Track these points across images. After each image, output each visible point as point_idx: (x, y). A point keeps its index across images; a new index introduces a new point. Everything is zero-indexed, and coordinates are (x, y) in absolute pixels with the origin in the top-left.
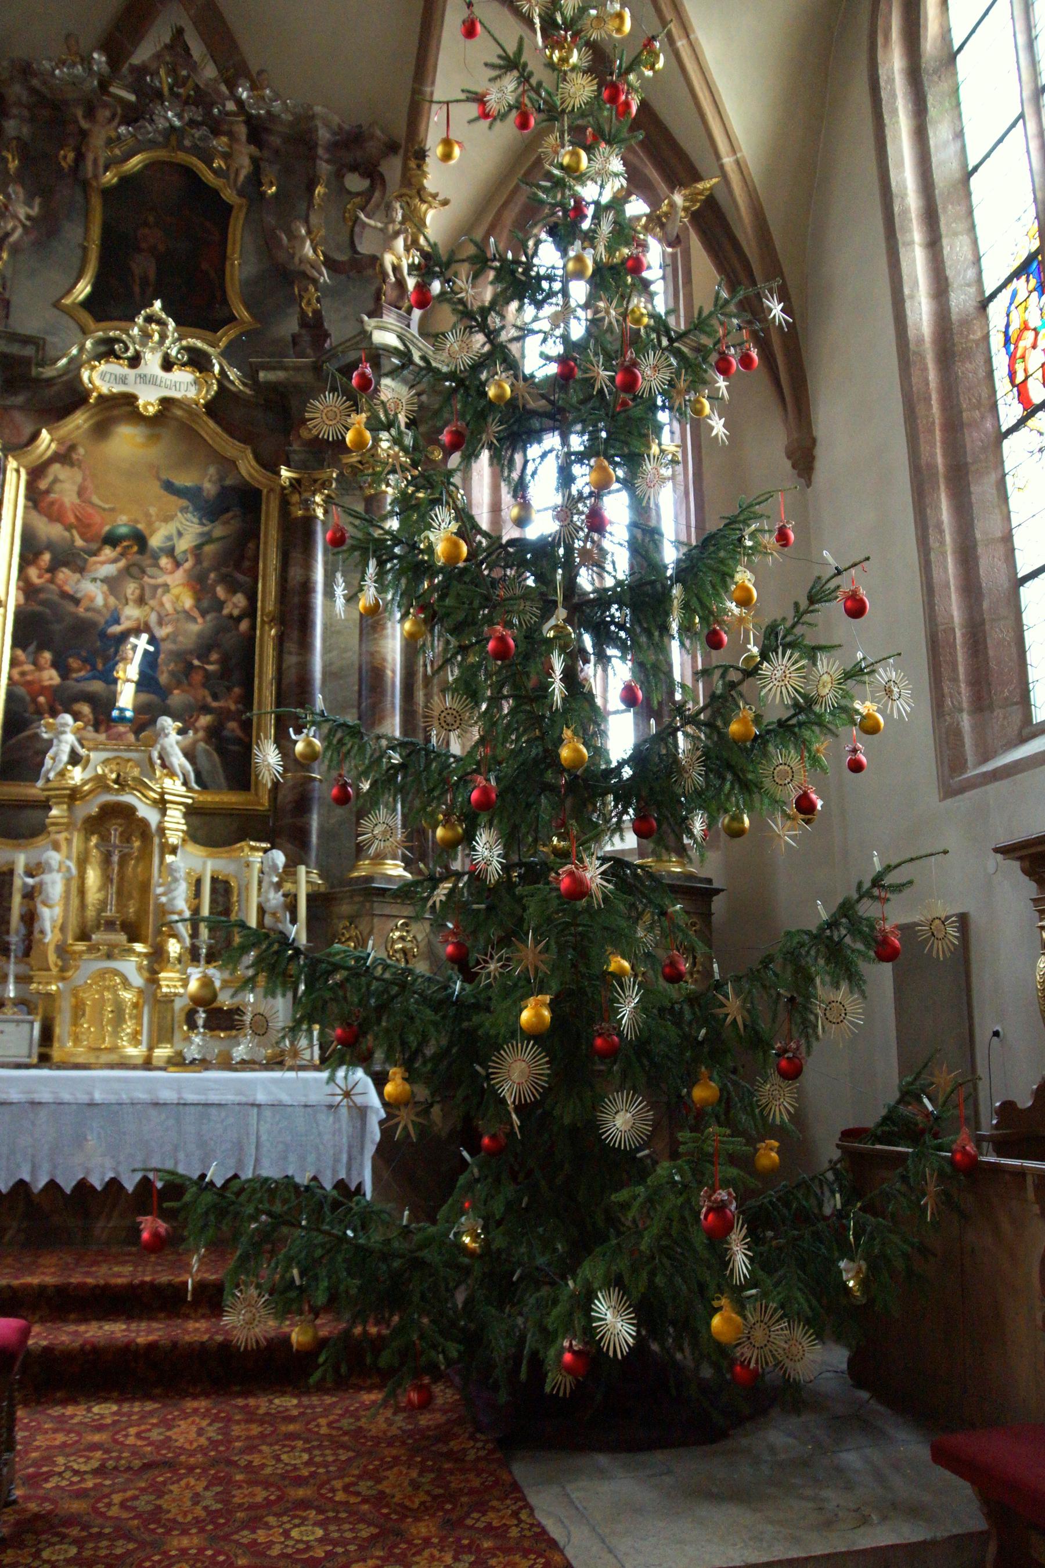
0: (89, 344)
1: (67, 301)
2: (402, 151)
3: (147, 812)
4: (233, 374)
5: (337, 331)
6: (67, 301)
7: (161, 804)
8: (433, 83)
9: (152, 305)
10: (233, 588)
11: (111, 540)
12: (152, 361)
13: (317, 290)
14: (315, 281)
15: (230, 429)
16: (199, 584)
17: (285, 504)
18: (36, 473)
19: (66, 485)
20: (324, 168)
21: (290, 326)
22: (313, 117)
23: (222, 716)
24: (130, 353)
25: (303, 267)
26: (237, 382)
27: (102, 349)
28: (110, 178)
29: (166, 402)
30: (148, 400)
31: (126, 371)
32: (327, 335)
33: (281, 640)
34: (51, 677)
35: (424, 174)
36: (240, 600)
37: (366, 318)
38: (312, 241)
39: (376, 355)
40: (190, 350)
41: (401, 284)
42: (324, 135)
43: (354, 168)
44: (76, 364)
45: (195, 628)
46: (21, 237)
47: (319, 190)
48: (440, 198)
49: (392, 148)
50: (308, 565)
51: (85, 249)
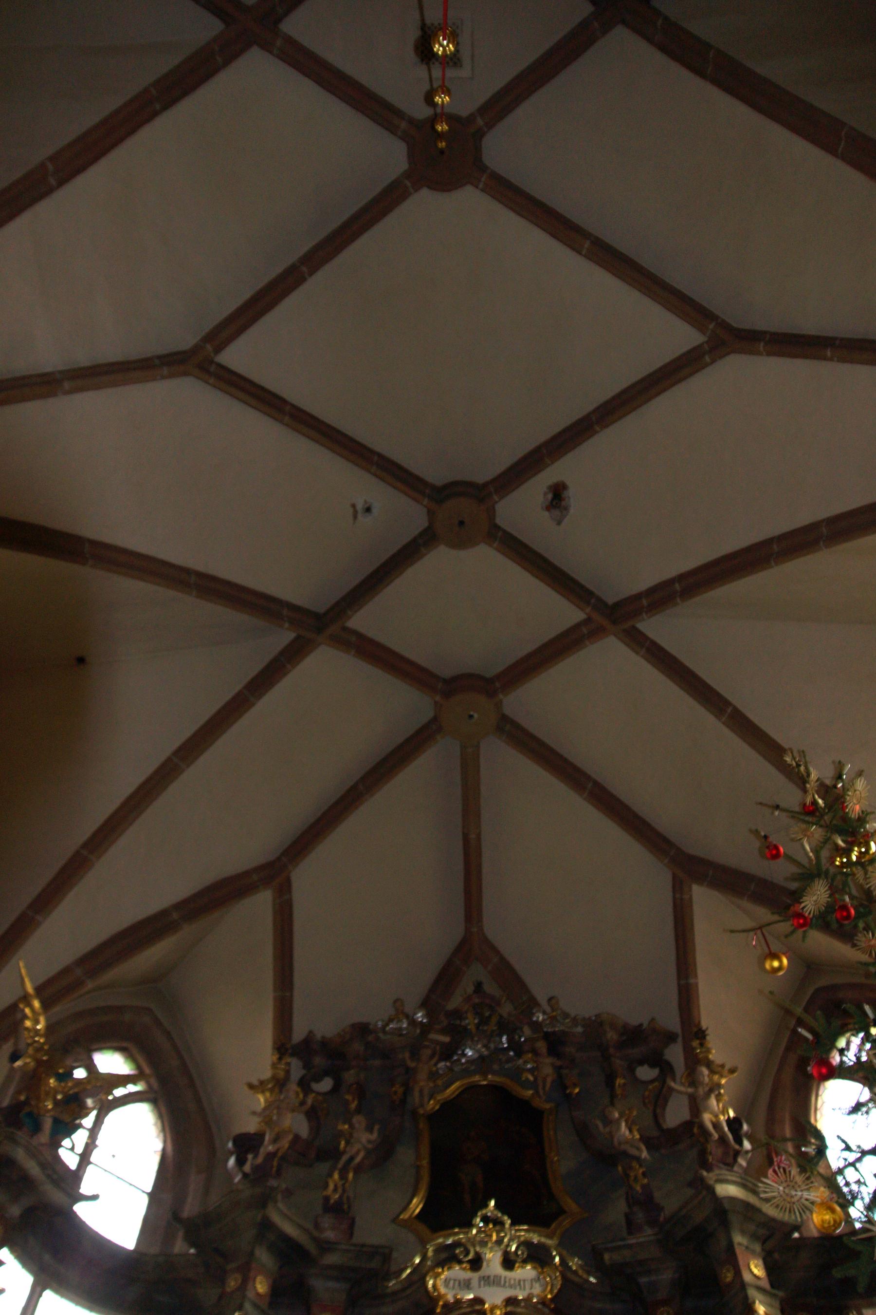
0: (430, 1253)
1: (405, 1216)
2: (680, 1039)
4: (574, 1263)
5: (671, 1199)
6: (405, 1216)
8: (696, 976)
9: (486, 1206)
13: (641, 1166)
14: (638, 1159)
20: (619, 1063)
21: (616, 1211)
22: (601, 1024)
24: (470, 1257)
25: (623, 1147)
26: (580, 1272)
27: (443, 1256)
28: (432, 1105)
30: (494, 1298)
31: (469, 1274)
32: (660, 1209)
35: (708, 1051)
37: (705, 1173)
38: (626, 1121)
39: (722, 1211)
40: (526, 1244)
41: (723, 1139)
42: (611, 1036)
43: (641, 1063)
44: (420, 1274)
46: (363, 1159)
47: (619, 1081)
48: (727, 1067)
49: (671, 1037)
51: (418, 1168)
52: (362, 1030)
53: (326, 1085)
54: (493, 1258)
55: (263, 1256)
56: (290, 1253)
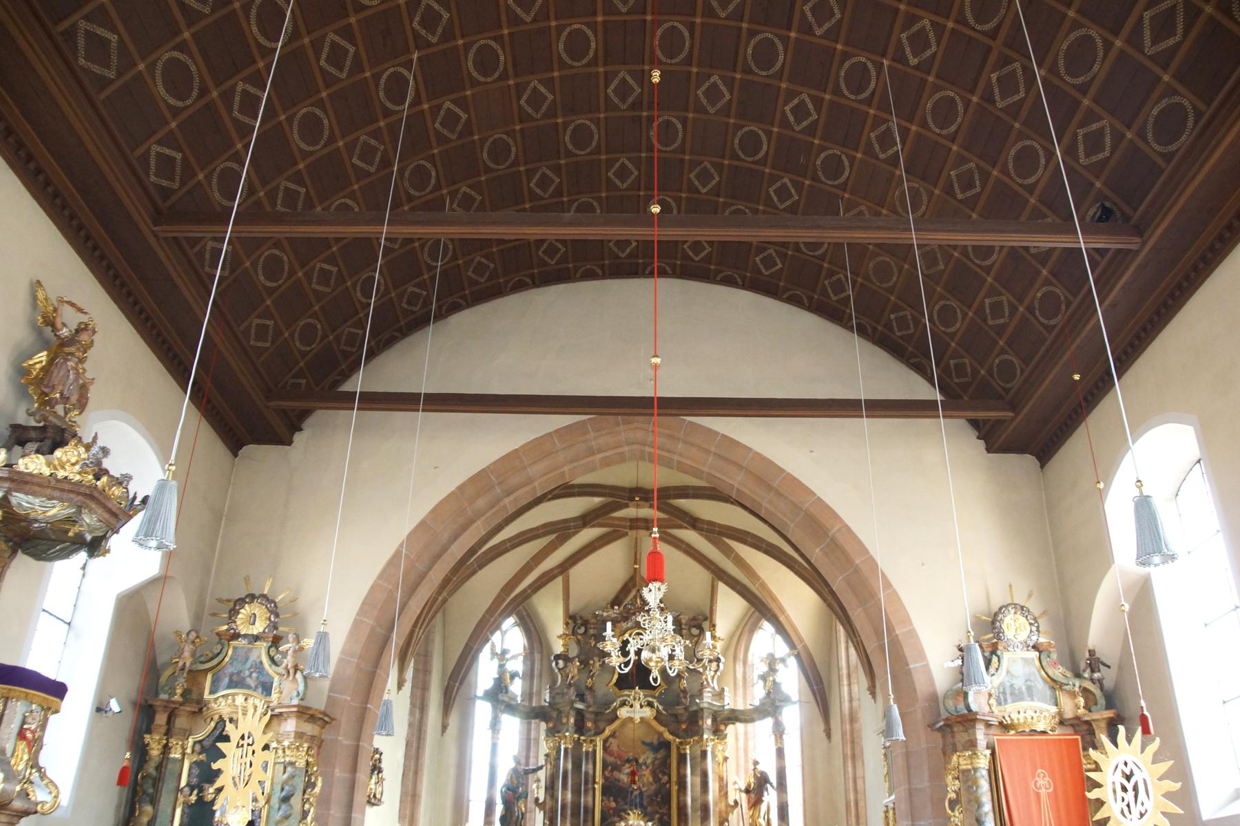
10: (664, 774)
11: (628, 761)
12: (637, 705)
15: (661, 724)
17: (678, 748)
18: (605, 741)
29: (642, 719)
30: (637, 718)
33: (679, 791)
34: (613, 805)
36: (666, 778)
42: (684, 621)
44: (615, 709)
49: (706, 619)
50: (685, 769)
52: (596, 616)
53: (582, 630)
54: (637, 705)
55: (572, 713)
56: (579, 713)
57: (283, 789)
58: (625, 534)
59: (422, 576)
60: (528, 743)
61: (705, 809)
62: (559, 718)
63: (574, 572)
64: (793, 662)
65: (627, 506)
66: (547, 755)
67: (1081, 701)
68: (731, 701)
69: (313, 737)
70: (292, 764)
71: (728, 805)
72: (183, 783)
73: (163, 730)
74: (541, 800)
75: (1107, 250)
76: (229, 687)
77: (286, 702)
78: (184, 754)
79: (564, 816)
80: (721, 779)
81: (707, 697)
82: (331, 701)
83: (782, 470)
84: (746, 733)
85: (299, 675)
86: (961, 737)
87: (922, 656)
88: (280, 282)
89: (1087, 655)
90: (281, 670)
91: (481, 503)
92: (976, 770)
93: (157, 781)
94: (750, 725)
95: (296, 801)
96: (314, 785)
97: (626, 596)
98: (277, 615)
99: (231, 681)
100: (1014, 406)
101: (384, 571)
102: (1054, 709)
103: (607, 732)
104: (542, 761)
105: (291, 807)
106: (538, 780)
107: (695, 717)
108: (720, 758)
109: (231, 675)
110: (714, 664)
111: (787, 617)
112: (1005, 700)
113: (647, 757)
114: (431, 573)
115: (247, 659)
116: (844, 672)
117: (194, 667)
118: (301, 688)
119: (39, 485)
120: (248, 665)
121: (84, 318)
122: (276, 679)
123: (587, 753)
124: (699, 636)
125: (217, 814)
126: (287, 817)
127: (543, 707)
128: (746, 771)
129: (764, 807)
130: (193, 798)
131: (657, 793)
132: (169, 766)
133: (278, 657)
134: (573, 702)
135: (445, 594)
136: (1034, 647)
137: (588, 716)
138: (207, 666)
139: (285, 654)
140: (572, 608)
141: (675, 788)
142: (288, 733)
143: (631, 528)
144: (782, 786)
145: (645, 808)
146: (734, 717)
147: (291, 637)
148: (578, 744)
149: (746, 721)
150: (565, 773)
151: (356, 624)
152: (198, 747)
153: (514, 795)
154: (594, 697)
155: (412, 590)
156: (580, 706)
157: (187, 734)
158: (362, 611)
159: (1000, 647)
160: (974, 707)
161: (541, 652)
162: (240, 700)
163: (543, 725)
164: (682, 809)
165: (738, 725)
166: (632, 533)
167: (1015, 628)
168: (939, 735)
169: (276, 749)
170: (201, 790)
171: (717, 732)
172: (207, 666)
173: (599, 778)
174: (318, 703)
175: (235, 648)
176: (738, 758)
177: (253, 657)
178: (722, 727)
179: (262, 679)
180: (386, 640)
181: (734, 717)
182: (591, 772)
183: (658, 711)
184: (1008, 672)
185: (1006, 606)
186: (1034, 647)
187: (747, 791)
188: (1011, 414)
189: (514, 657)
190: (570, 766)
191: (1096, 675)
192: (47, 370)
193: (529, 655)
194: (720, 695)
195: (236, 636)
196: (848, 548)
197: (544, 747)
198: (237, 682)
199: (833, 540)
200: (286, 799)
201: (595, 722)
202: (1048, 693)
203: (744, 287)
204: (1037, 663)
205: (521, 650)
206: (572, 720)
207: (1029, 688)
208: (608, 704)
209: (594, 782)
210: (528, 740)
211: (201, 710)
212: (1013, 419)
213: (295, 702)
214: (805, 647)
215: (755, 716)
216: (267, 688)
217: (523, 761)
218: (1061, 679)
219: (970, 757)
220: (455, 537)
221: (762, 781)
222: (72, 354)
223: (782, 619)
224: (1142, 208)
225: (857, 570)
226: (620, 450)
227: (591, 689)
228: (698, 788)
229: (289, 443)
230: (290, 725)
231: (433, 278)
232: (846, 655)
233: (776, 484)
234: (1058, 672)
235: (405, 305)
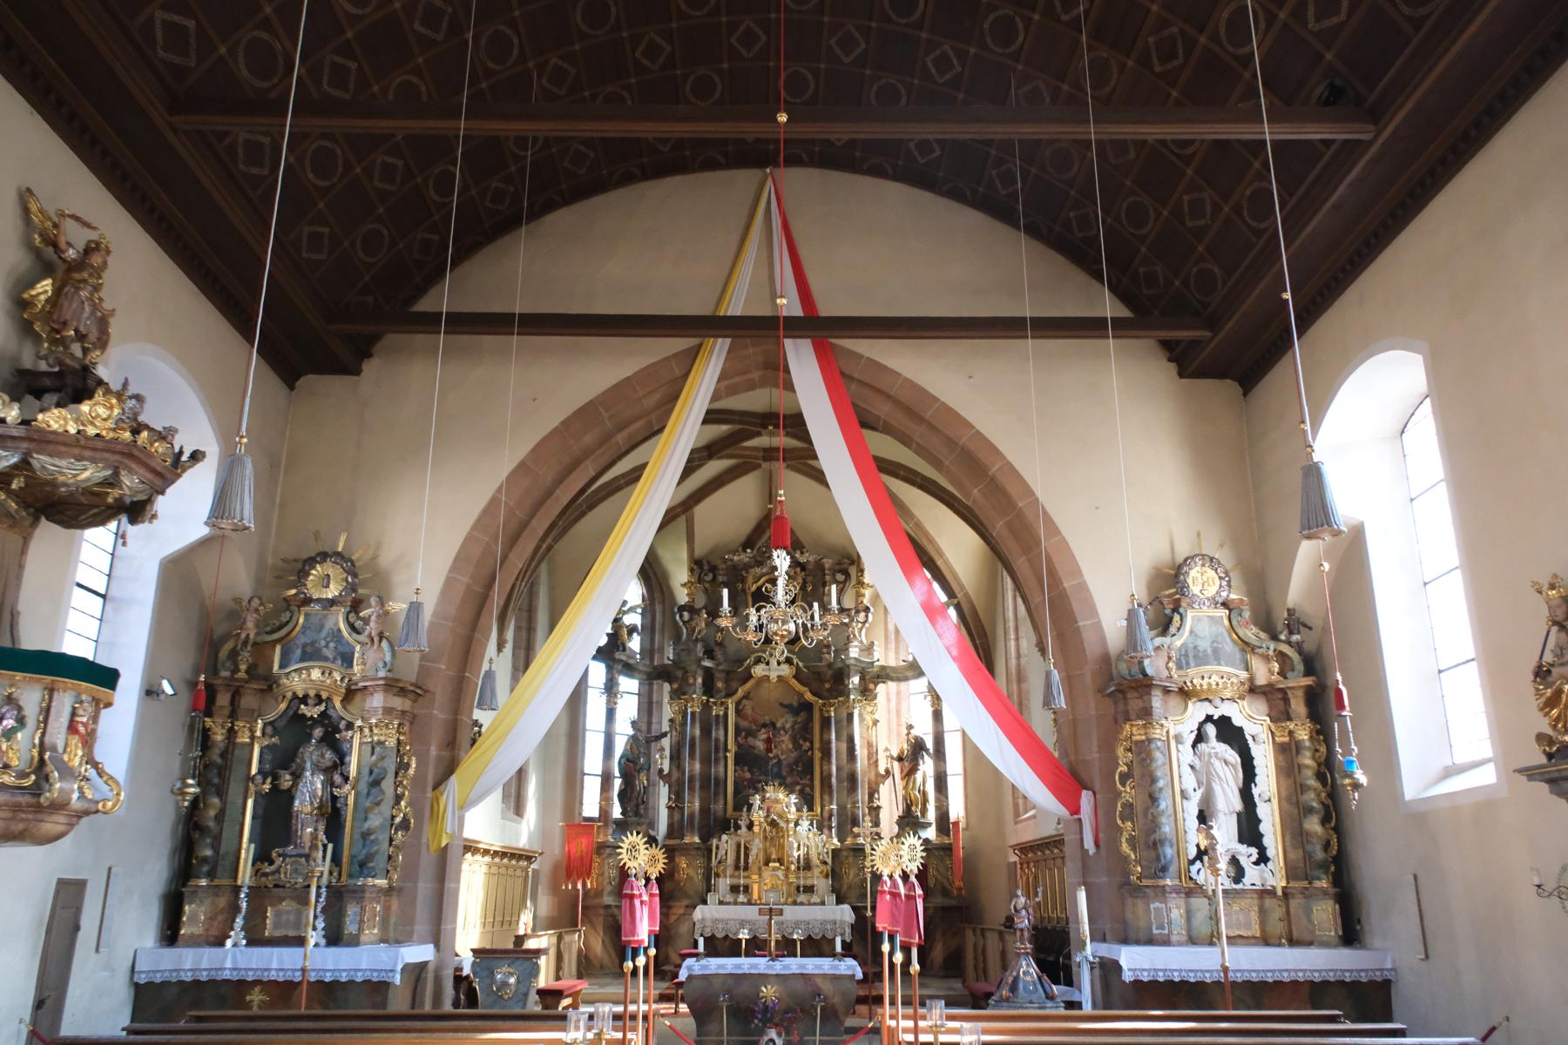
3: (782, 824)
7: (788, 822)
10: (805, 740)
11: (764, 726)
12: (774, 662)
16: (794, 740)
18: (738, 703)
19: (748, 706)
20: (828, 578)
23: (804, 786)
28: (754, 588)
30: (773, 676)
33: (822, 759)
34: (748, 775)
45: (793, 755)
49: (852, 563)
52: (725, 561)
53: (710, 576)
55: (700, 672)
57: (371, 772)
58: (759, 466)
59: (523, 526)
60: (648, 706)
61: (852, 779)
62: (685, 679)
63: (700, 511)
64: (952, 612)
65: (759, 434)
66: (671, 721)
67: (1276, 667)
68: (883, 656)
69: (403, 712)
70: (381, 743)
71: (878, 774)
72: (254, 771)
73: (227, 712)
74: (666, 771)
75: (1333, 141)
76: (302, 660)
77: (371, 673)
78: (253, 738)
79: (691, 789)
80: (870, 745)
81: (854, 652)
82: (424, 671)
83: (937, 400)
84: (898, 693)
85: (384, 644)
86: (1135, 704)
87: (1093, 611)
88: (335, 180)
89: (1286, 615)
90: (362, 638)
91: (588, 439)
92: (1150, 741)
93: (224, 770)
94: (903, 685)
95: (388, 785)
96: (408, 766)
97: (760, 537)
98: (355, 575)
99: (304, 652)
100: (1213, 324)
101: (478, 521)
102: (1244, 675)
103: (740, 693)
104: (666, 727)
105: (383, 792)
106: (662, 749)
107: (840, 676)
108: (869, 719)
109: (304, 646)
110: (862, 615)
111: (947, 562)
112: (1188, 664)
113: (786, 721)
114: (534, 522)
115: (322, 627)
116: (1011, 624)
117: (259, 639)
118: (388, 658)
119: (65, 444)
120: (324, 634)
121: (93, 236)
122: (358, 648)
123: (717, 716)
124: (844, 582)
125: (297, 803)
126: (378, 804)
127: (666, 666)
128: (899, 734)
129: (919, 776)
130: (267, 787)
131: (796, 762)
132: (237, 752)
133: (358, 624)
134: (700, 660)
135: (549, 540)
136: (1224, 604)
137: (717, 675)
138: (276, 636)
139: (366, 621)
140: (698, 552)
141: (818, 755)
142: (375, 710)
143: (765, 459)
144: (939, 754)
145: (784, 778)
146: (884, 675)
147: (373, 601)
148: (706, 706)
149: (899, 680)
150: (693, 739)
151: (449, 583)
152: (269, 730)
153: (632, 767)
154: (724, 653)
155: (512, 541)
156: (707, 663)
157: (253, 715)
158: (456, 567)
159: (1183, 604)
160: (1149, 671)
161: (663, 603)
162: (316, 674)
163: (667, 687)
164: (825, 781)
165: (890, 683)
166: (765, 465)
167: (1203, 582)
168: (1109, 701)
169: (361, 729)
170: (276, 777)
171: (866, 692)
172: (276, 636)
173: (731, 745)
174: (409, 674)
175: (307, 615)
176: (889, 721)
177: (329, 624)
178: (871, 686)
179: (341, 648)
180: (484, 599)
181: (884, 675)
182: (722, 738)
183: (797, 667)
184: (1191, 632)
185: (1192, 558)
186: (1224, 604)
187: (900, 759)
188: (1208, 334)
189: (632, 609)
190: (697, 732)
191: (1296, 638)
192: (55, 301)
193: (648, 609)
194: (869, 648)
195: (308, 601)
196: (1013, 490)
197: (668, 711)
198: (311, 654)
199: (992, 479)
200: (376, 783)
201: (726, 681)
202: (1238, 656)
203: (896, 178)
204: (1226, 622)
205: (639, 601)
206: (700, 680)
207: (1216, 651)
208: (741, 661)
209: (726, 750)
210: (650, 703)
211: (270, 688)
212: (1212, 339)
213: (382, 674)
214: (966, 595)
215: (909, 674)
216: (347, 660)
217: (644, 727)
218: (1252, 639)
219: (1145, 726)
220: (560, 480)
221: (918, 747)
222: (84, 281)
223: (939, 563)
224: (1379, 88)
225: (1020, 515)
226: (749, 376)
227: (720, 644)
228: (844, 756)
229: (357, 372)
230: (377, 701)
231: (522, 170)
232: (1012, 606)
233: (928, 415)
234: (1251, 633)
235: (488, 204)
